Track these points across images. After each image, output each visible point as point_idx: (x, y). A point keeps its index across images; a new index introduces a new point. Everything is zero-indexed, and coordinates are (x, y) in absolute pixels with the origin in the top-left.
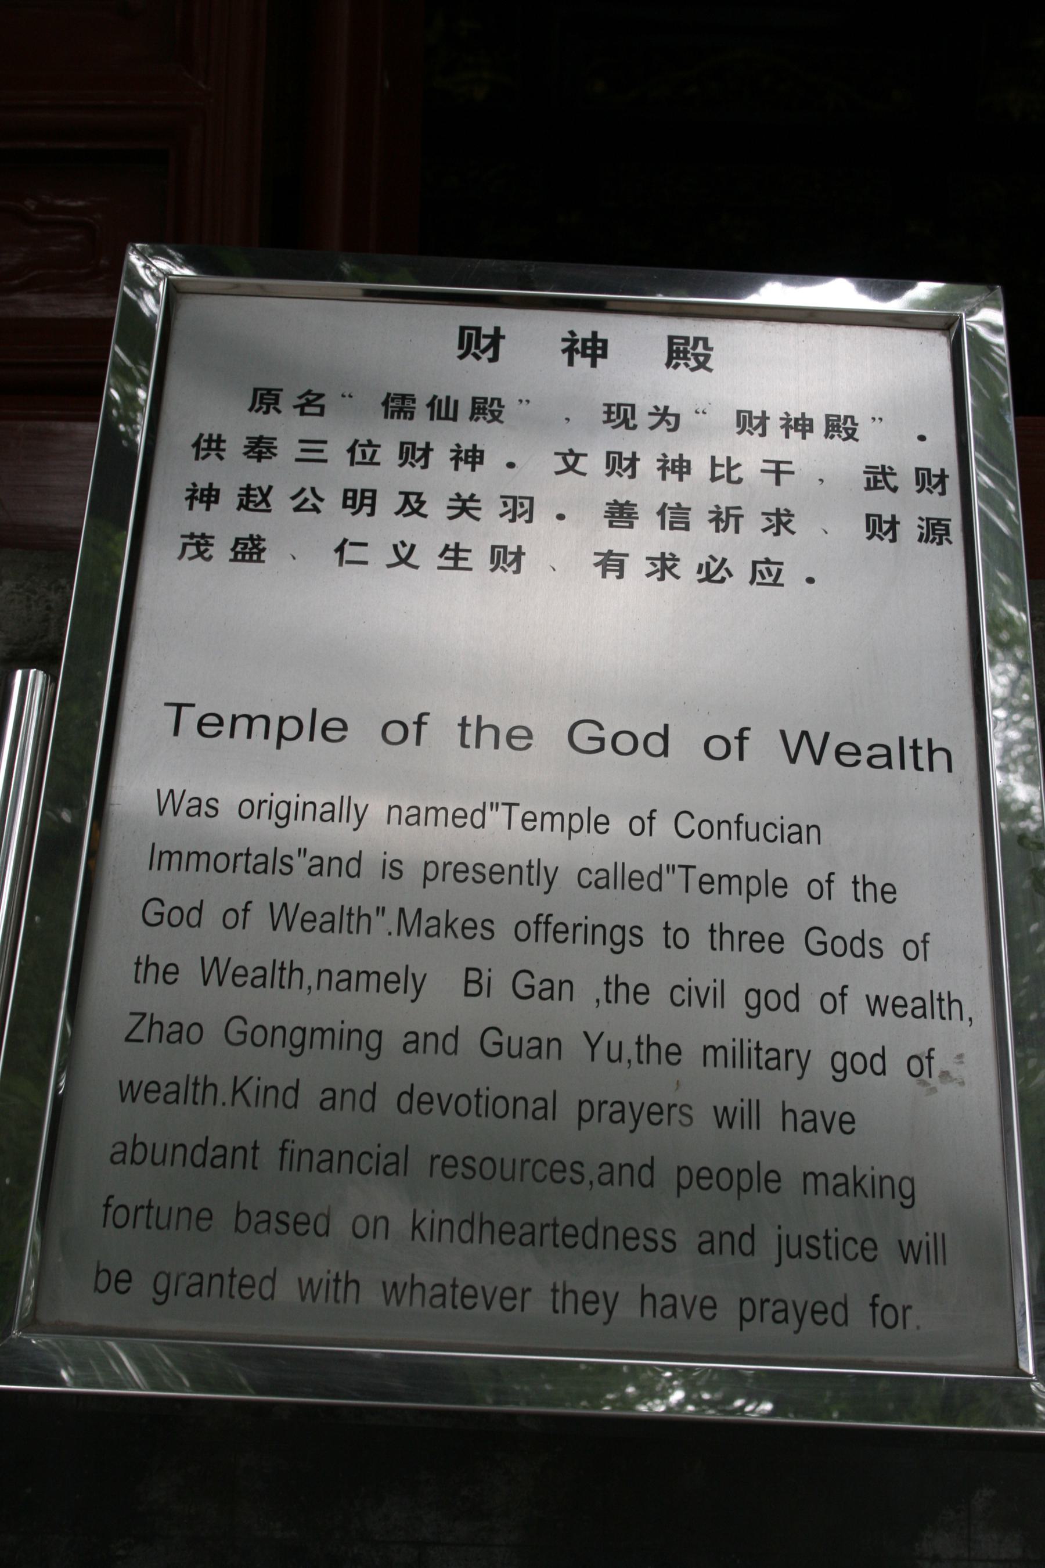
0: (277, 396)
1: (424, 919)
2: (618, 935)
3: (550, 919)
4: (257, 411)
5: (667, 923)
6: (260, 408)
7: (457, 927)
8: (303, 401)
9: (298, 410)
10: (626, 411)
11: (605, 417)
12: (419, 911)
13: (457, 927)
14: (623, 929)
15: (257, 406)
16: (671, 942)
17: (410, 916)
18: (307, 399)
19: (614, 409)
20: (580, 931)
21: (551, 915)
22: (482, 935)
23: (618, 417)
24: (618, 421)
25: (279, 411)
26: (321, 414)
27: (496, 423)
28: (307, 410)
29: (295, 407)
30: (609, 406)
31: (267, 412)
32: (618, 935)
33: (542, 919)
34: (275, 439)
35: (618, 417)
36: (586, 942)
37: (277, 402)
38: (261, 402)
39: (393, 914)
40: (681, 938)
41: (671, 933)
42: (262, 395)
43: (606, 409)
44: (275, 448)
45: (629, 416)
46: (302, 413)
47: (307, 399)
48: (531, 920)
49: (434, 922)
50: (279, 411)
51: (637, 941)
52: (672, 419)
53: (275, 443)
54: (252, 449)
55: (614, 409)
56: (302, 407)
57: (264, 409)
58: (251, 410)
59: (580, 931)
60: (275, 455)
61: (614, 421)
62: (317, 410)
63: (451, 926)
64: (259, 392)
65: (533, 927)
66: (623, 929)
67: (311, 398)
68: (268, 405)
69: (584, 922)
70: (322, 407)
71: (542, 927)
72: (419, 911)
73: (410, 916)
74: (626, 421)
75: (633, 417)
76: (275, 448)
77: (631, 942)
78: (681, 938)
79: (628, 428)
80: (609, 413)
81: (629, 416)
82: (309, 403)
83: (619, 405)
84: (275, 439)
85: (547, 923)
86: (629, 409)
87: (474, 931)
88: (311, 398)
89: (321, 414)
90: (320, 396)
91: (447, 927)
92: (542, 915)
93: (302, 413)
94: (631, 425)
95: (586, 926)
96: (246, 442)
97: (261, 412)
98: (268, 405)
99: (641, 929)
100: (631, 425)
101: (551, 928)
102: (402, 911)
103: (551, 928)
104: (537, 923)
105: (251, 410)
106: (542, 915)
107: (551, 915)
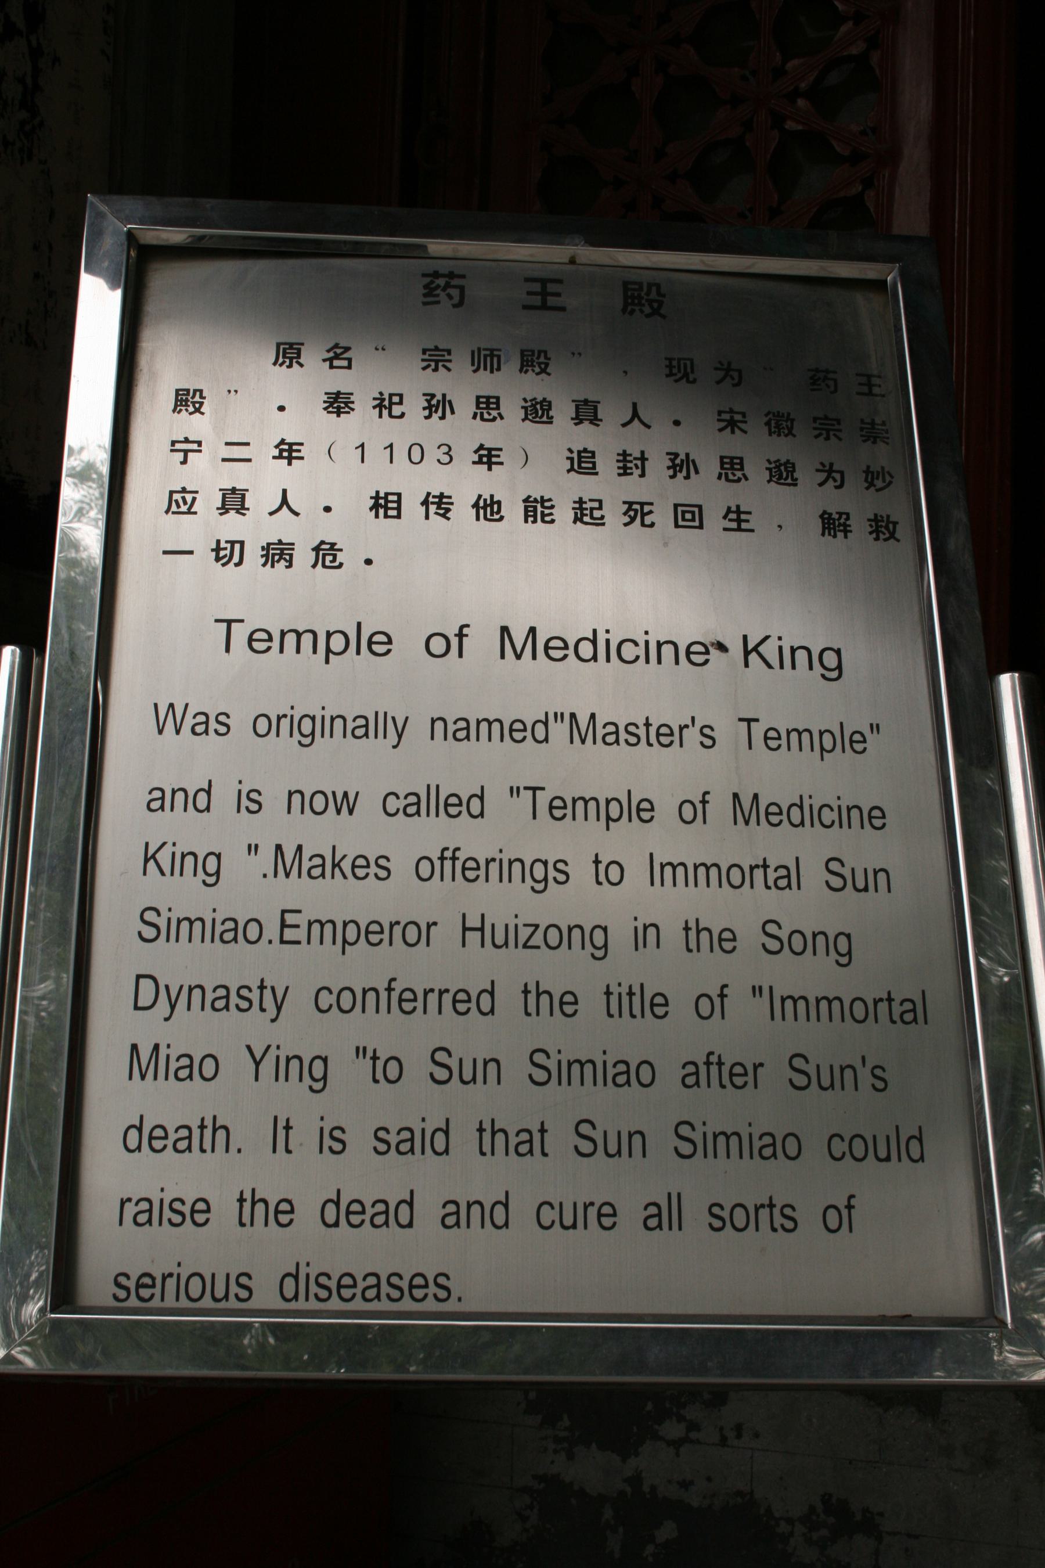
0: (299, 350)
1: (306, 856)
2: (539, 871)
3: (457, 854)
4: (281, 365)
5: (597, 855)
6: (284, 362)
7: (346, 865)
8: (331, 354)
9: (328, 363)
10: (685, 365)
11: (667, 371)
12: (300, 848)
13: (346, 865)
14: (545, 863)
15: (281, 360)
16: (602, 878)
17: (289, 853)
18: (335, 353)
19: (675, 363)
20: (494, 867)
21: (458, 849)
22: (376, 875)
23: (679, 371)
24: (679, 375)
25: (301, 365)
26: (349, 367)
27: (543, 375)
28: (336, 363)
29: (324, 360)
30: (670, 360)
31: (290, 366)
32: (539, 871)
33: (448, 854)
34: (352, 394)
35: (679, 371)
36: (501, 881)
37: (299, 357)
38: (284, 357)
39: (267, 853)
40: (614, 873)
41: (602, 868)
42: (284, 349)
43: (667, 363)
44: (353, 402)
45: (689, 370)
46: (331, 367)
47: (335, 353)
48: (435, 856)
49: (318, 861)
50: (301, 365)
51: (561, 878)
52: (735, 375)
53: (352, 398)
54: (331, 404)
55: (675, 363)
56: (331, 360)
57: (287, 363)
58: (275, 364)
59: (494, 867)
60: (353, 410)
61: (675, 375)
62: (345, 363)
63: (338, 865)
64: (282, 347)
65: (437, 864)
66: (545, 863)
67: (339, 351)
68: (291, 359)
69: (498, 856)
70: (350, 360)
71: (448, 864)
72: (300, 848)
73: (289, 853)
74: (686, 375)
75: (692, 372)
76: (353, 402)
77: (555, 879)
78: (614, 873)
79: (688, 381)
80: (670, 367)
81: (689, 370)
82: (337, 357)
83: (679, 360)
84: (352, 394)
85: (454, 859)
86: (688, 363)
87: (366, 870)
88: (339, 351)
89: (349, 367)
90: (347, 349)
91: (334, 866)
92: (447, 849)
93: (331, 367)
94: (691, 379)
95: (501, 860)
96: (325, 398)
97: (284, 366)
98: (291, 359)
99: (566, 864)
100: (691, 379)
101: (459, 865)
102: (279, 847)
103: (459, 865)
104: (442, 858)
105: (275, 364)
106: (447, 849)
107: (458, 849)
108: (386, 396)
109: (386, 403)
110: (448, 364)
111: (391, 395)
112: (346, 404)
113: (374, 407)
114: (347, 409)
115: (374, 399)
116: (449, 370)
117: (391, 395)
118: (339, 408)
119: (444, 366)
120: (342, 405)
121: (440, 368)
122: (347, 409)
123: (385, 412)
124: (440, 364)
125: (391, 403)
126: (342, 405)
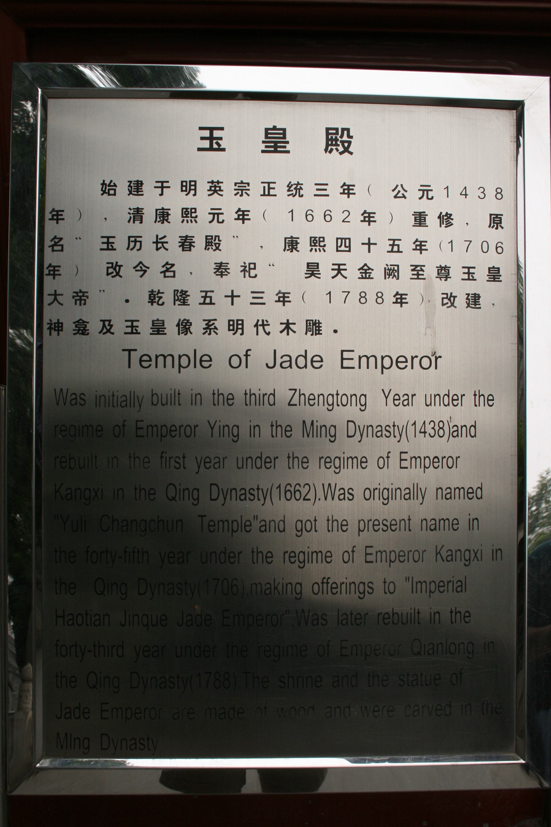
44: (229, 269)
60: (229, 273)
76: (229, 269)
108: (247, 265)
109: (247, 269)
110: (248, 192)
111: (250, 264)
112: (225, 269)
113: (241, 271)
114: (226, 273)
115: (242, 266)
116: (248, 195)
117: (250, 264)
118: (222, 272)
119: (246, 193)
120: (224, 271)
121: (244, 194)
122: (226, 273)
123: (247, 274)
124: (244, 192)
125: (250, 269)
126: (224, 271)
